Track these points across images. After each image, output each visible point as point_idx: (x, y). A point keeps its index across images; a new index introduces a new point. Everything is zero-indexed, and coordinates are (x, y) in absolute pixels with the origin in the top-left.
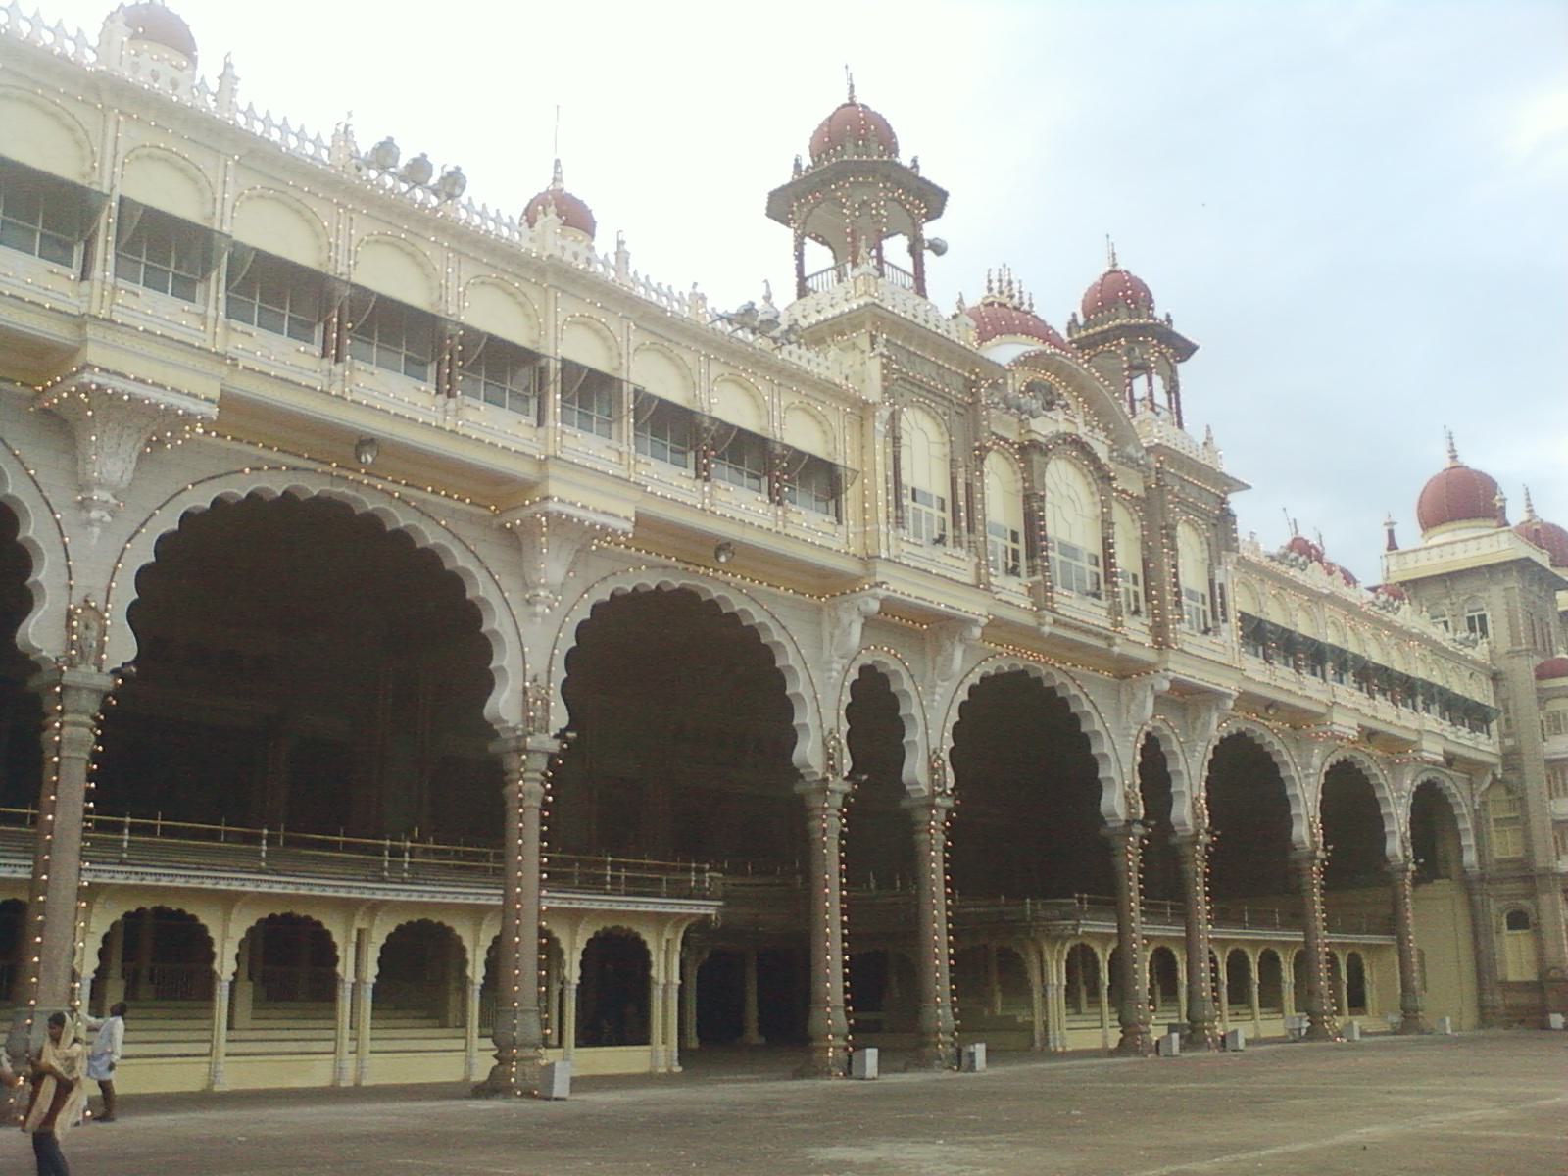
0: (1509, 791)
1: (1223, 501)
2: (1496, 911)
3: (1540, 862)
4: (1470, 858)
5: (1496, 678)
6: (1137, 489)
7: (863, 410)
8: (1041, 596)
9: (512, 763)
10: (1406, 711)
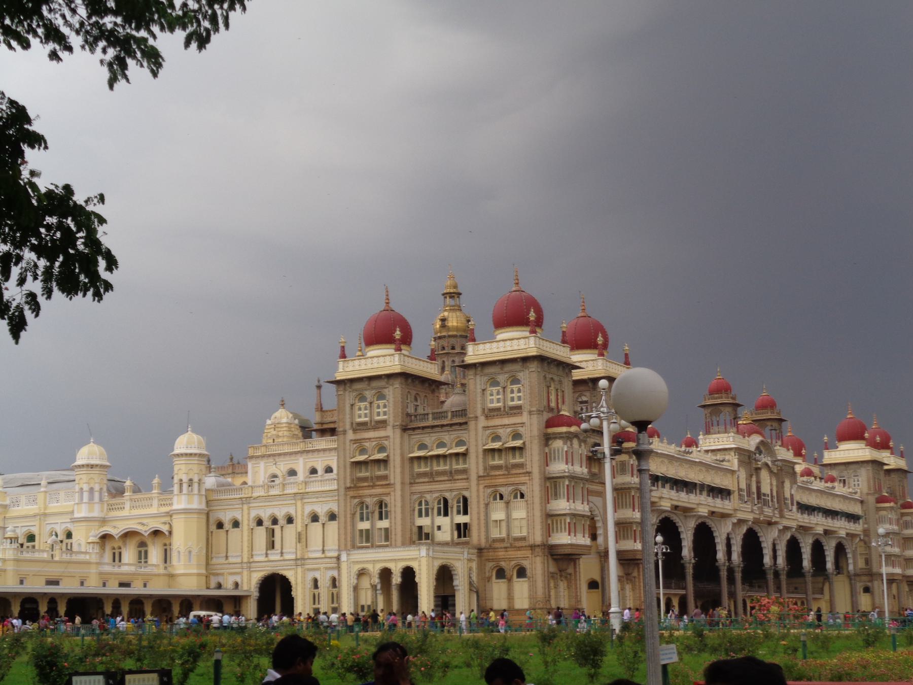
0: (865, 543)
1: (793, 469)
2: (859, 586)
3: (875, 570)
4: (851, 567)
5: (862, 502)
6: (775, 471)
7: (733, 472)
8: (761, 509)
9: (688, 565)
10: (835, 521)
